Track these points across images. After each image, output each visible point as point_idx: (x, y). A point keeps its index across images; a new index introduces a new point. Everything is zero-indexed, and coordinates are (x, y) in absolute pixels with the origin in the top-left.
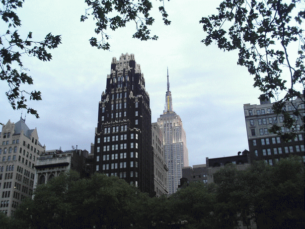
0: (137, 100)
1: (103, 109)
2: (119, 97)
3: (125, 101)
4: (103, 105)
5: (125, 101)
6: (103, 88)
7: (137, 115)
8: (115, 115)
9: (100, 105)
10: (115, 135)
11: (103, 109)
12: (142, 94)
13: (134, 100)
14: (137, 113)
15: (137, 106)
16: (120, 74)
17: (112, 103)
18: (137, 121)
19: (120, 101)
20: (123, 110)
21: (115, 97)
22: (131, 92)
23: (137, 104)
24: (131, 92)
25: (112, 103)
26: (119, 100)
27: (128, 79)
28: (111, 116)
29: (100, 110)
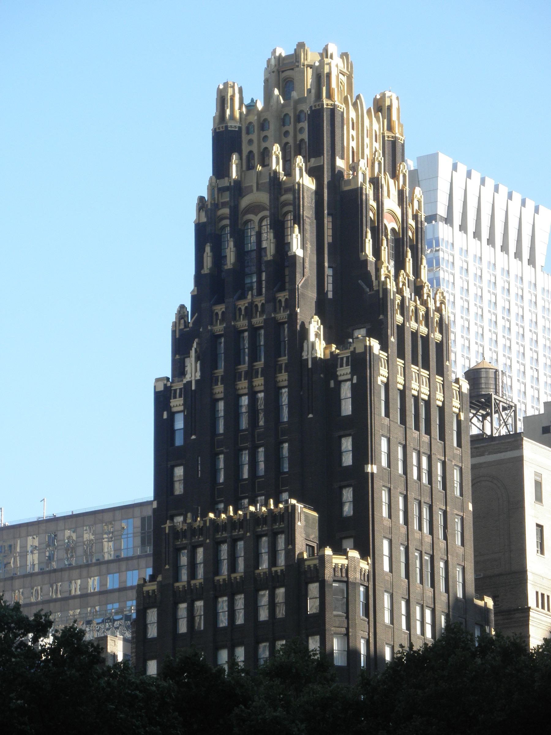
0: (344, 371)
2: (254, 357)
3: (283, 377)
4: (177, 404)
5: (283, 377)
6: (176, 283)
8: (234, 467)
9: (162, 399)
10: (231, 590)
15: (347, 408)
16: (255, 208)
17: (219, 389)
18: (348, 494)
19: (259, 382)
20: (275, 434)
21: (235, 358)
25: (219, 389)
26: (251, 375)
28: (214, 472)
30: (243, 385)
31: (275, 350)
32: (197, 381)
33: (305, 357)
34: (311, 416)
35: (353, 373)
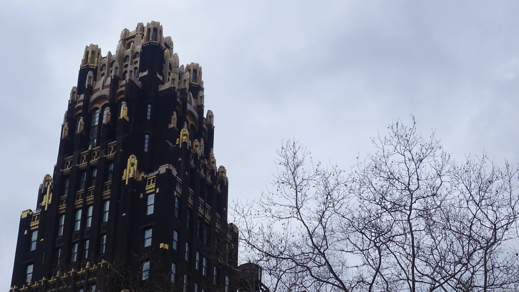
1: (35, 236)
4: (35, 224)
5: (107, 193)
7: (148, 243)
9: (25, 223)
11: (35, 236)
12: (176, 165)
13: (137, 185)
14: (149, 233)
17: (63, 207)
19: (90, 198)
22: (132, 160)
23: (151, 200)
24: (132, 160)
25: (63, 207)
27: (123, 113)
29: (23, 242)
30: (80, 201)
31: (104, 175)
32: (49, 205)
33: (124, 179)
34: (124, 214)
35: (155, 188)
